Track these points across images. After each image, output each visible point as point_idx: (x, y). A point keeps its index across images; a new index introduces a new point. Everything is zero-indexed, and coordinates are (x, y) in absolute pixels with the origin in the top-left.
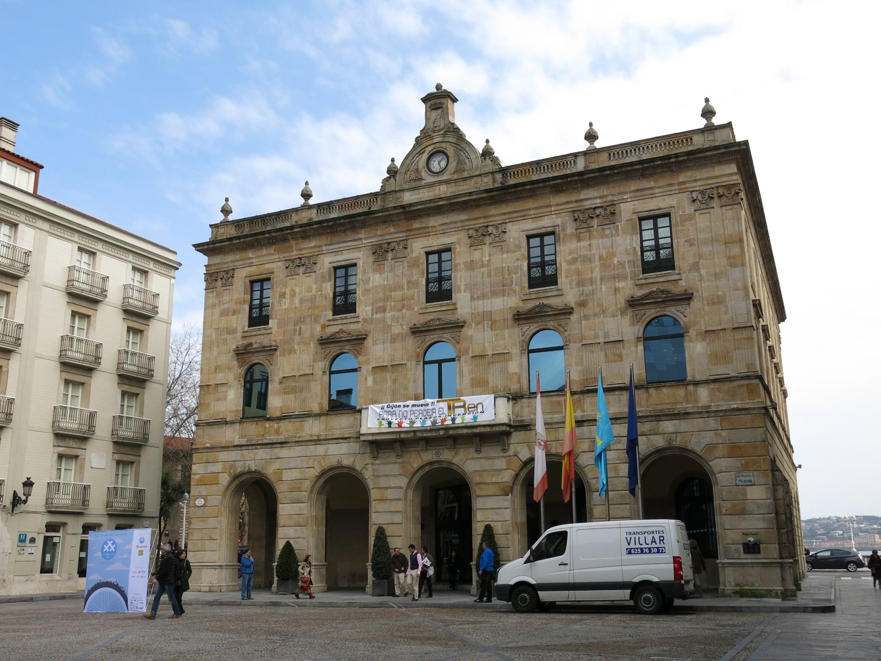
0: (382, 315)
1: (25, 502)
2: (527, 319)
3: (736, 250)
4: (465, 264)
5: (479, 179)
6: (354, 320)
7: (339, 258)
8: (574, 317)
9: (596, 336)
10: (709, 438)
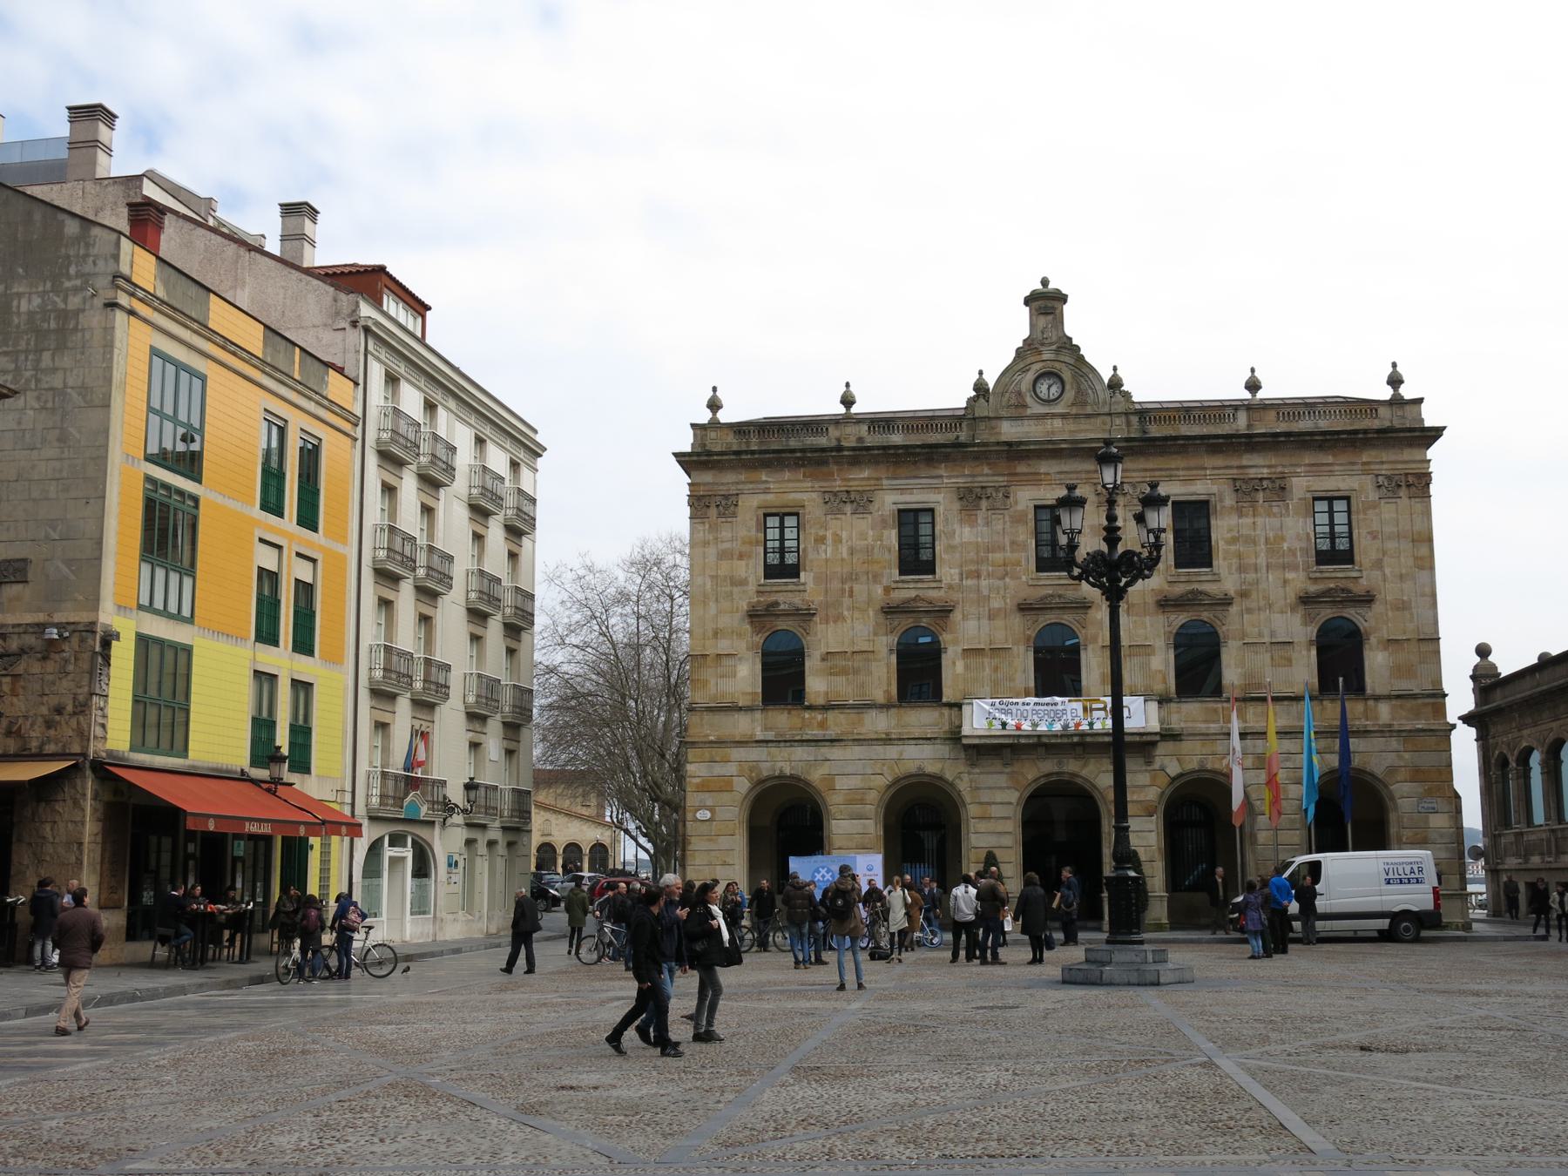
3: (1423, 551)
5: (1108, 419)
7: (907, 498)
8: (1234, 609)
10: (1390, 759)
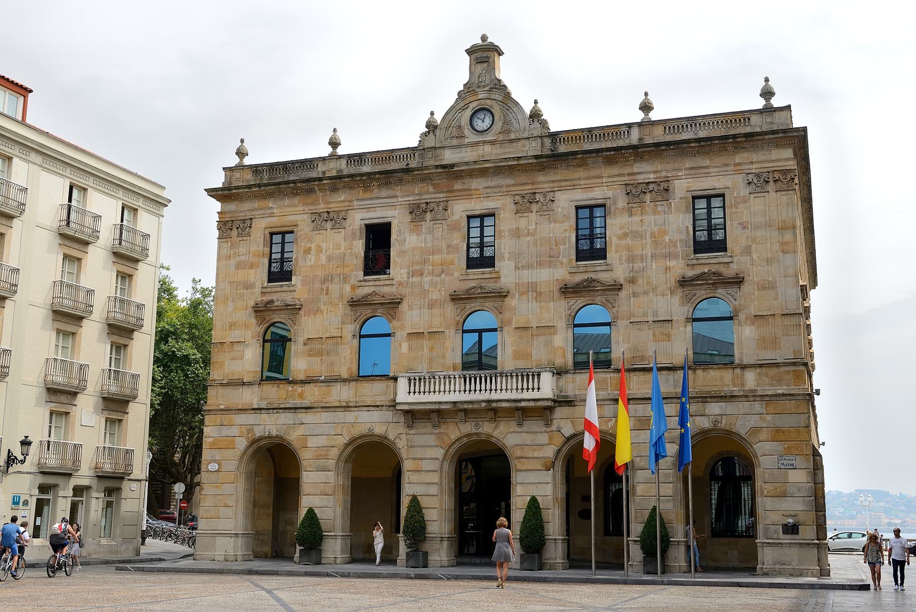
1: (23, 462)
2: (574, 292)
3: (788, 237)
4: (510, 230)
6: (388, 282)
8: (623, 294)
9: (645, 314)
10: (754, 421)
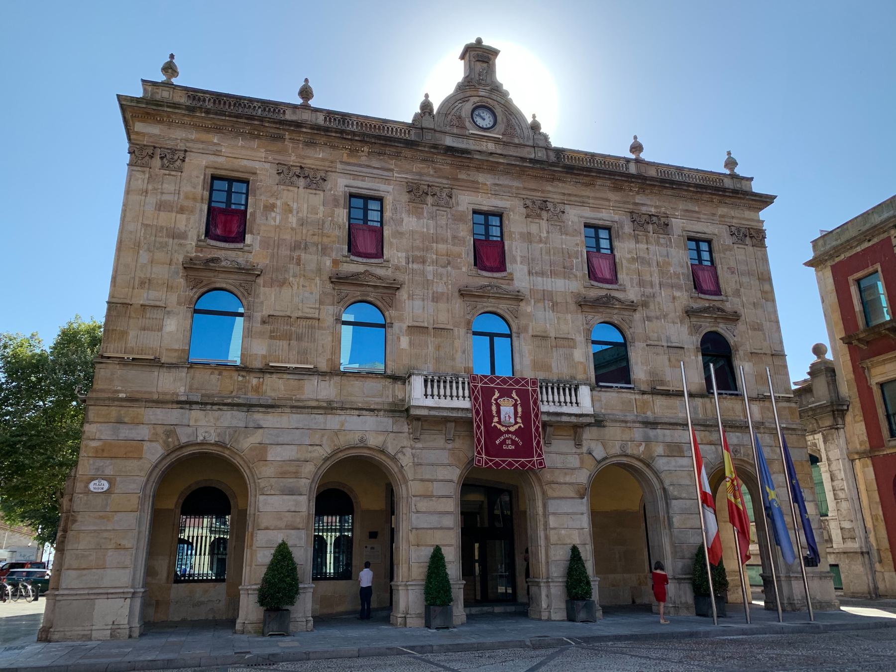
0: (420, 266)
4: (521, 234)
7: (359, 183)
8: (637, 316)
